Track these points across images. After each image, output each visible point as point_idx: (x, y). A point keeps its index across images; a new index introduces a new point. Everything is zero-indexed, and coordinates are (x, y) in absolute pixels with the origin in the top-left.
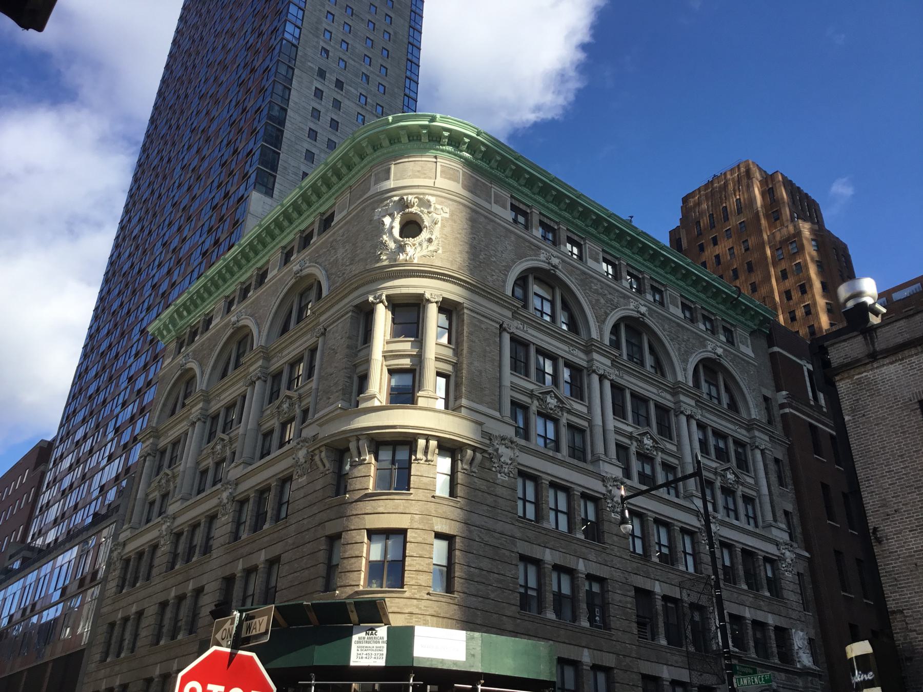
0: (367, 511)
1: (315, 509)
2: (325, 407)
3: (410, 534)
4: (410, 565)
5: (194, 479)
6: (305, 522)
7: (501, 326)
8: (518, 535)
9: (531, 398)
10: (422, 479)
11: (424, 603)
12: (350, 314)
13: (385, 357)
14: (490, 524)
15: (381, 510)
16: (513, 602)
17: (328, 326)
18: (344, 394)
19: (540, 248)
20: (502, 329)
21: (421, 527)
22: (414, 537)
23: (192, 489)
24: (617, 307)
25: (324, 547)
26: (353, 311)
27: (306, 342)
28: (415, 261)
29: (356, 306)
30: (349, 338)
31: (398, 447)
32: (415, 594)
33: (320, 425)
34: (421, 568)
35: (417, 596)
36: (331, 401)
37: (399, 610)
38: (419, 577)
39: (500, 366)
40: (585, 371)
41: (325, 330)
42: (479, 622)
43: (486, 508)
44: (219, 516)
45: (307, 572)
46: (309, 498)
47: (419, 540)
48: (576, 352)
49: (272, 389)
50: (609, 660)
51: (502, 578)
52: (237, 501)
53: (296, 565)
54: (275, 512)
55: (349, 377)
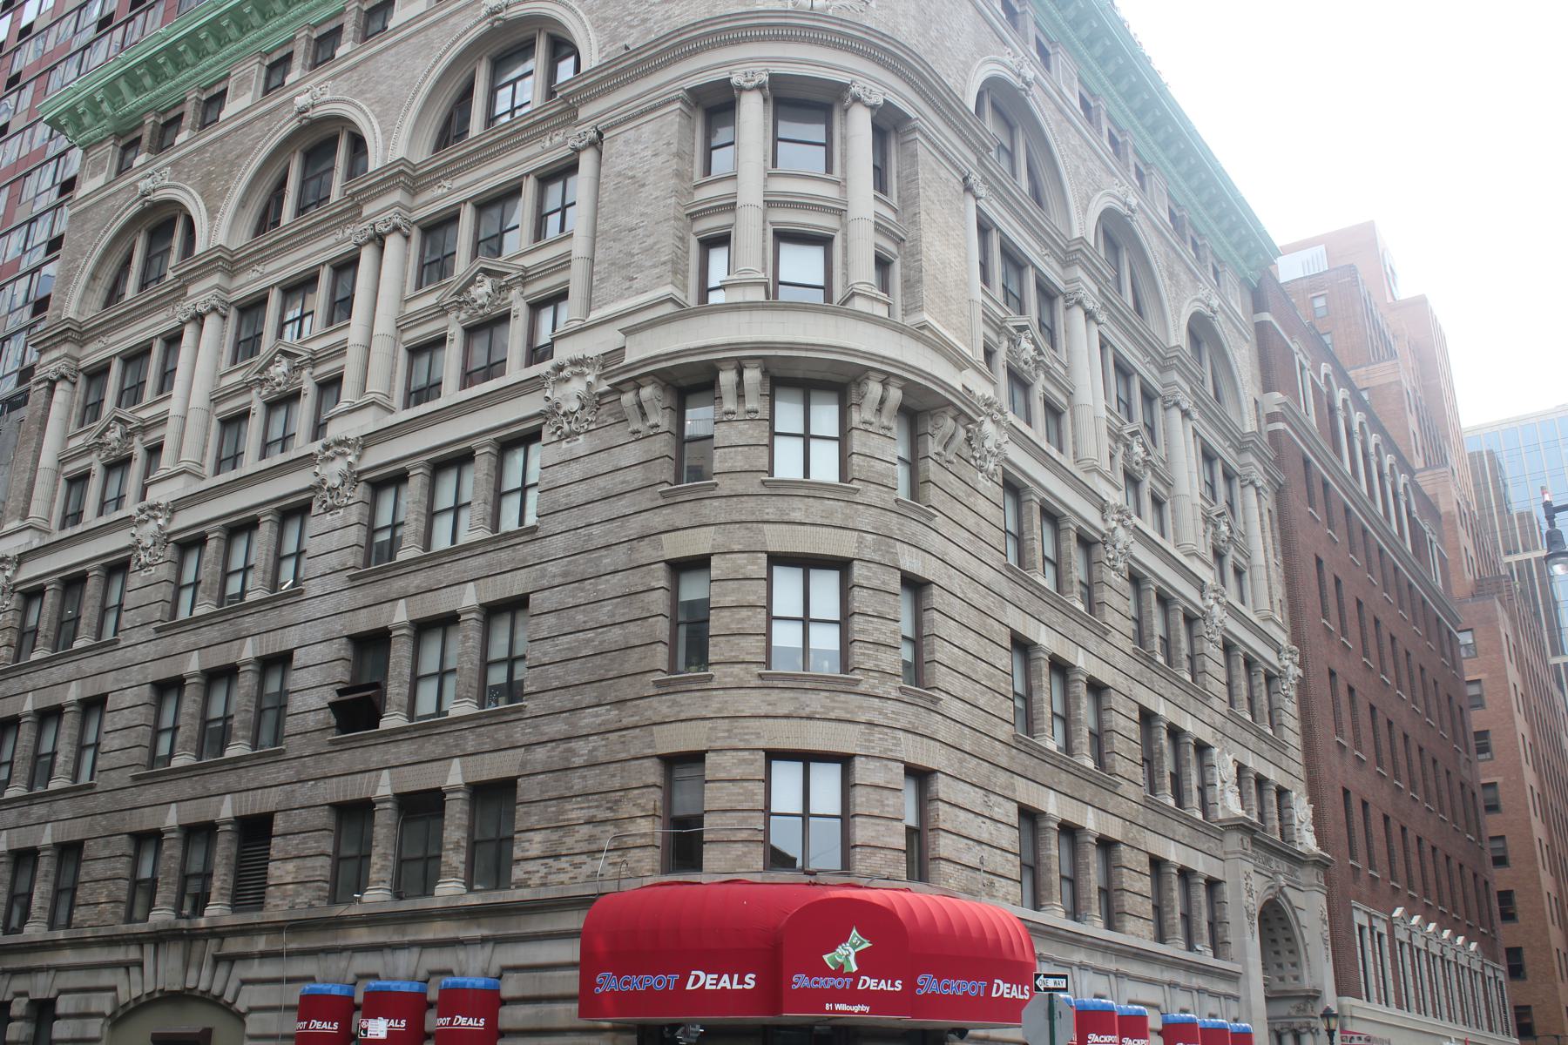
0: (766, 517)
1: (622, 506)
2: (621, 297)
3: (858, 571)
4: (863, 631)
5: (207, 434)
6: (595, 530)
7: (965, 179)
8: (1007, 594)
9: (998, 334)
10: (873, 462)
11: (890, 706)
12: (678, 105)
13: (769, 204)
14: (973, 566)
15: (797, 516)
16: (1005, 717)
17: (608, 128)
18: (675, 272)
19: (1005, 43)
20: (968, 189)
21: (877, 558)
22: (868, 578)
23: (204, 454)
24: (1099, 189)
25: (662, 583)
26: (683, 101)
27: (529, 159)
28: (830, 12)
29: (690, 91)
31: (814, 396)
32: (873, 687)
33: (627, 332)
34: (882, 639)
35: (879, 692)
36: (636, 284)
37: (848, 716)
38: (881, 655)
39: (967, 261)
40: (1061, 300)
41: (600, 135)
42: (967, 749)
43: (967, 535)
44: (315, 510)
45: (617, 631)
46: (600, 482)
47: (876, 583)
48: (1051, 260)
49: (422, 256)
50: (1114, 830)
51: (992, 670)
53: (580, 617)
54: (489, 509)
55: (682, 239)
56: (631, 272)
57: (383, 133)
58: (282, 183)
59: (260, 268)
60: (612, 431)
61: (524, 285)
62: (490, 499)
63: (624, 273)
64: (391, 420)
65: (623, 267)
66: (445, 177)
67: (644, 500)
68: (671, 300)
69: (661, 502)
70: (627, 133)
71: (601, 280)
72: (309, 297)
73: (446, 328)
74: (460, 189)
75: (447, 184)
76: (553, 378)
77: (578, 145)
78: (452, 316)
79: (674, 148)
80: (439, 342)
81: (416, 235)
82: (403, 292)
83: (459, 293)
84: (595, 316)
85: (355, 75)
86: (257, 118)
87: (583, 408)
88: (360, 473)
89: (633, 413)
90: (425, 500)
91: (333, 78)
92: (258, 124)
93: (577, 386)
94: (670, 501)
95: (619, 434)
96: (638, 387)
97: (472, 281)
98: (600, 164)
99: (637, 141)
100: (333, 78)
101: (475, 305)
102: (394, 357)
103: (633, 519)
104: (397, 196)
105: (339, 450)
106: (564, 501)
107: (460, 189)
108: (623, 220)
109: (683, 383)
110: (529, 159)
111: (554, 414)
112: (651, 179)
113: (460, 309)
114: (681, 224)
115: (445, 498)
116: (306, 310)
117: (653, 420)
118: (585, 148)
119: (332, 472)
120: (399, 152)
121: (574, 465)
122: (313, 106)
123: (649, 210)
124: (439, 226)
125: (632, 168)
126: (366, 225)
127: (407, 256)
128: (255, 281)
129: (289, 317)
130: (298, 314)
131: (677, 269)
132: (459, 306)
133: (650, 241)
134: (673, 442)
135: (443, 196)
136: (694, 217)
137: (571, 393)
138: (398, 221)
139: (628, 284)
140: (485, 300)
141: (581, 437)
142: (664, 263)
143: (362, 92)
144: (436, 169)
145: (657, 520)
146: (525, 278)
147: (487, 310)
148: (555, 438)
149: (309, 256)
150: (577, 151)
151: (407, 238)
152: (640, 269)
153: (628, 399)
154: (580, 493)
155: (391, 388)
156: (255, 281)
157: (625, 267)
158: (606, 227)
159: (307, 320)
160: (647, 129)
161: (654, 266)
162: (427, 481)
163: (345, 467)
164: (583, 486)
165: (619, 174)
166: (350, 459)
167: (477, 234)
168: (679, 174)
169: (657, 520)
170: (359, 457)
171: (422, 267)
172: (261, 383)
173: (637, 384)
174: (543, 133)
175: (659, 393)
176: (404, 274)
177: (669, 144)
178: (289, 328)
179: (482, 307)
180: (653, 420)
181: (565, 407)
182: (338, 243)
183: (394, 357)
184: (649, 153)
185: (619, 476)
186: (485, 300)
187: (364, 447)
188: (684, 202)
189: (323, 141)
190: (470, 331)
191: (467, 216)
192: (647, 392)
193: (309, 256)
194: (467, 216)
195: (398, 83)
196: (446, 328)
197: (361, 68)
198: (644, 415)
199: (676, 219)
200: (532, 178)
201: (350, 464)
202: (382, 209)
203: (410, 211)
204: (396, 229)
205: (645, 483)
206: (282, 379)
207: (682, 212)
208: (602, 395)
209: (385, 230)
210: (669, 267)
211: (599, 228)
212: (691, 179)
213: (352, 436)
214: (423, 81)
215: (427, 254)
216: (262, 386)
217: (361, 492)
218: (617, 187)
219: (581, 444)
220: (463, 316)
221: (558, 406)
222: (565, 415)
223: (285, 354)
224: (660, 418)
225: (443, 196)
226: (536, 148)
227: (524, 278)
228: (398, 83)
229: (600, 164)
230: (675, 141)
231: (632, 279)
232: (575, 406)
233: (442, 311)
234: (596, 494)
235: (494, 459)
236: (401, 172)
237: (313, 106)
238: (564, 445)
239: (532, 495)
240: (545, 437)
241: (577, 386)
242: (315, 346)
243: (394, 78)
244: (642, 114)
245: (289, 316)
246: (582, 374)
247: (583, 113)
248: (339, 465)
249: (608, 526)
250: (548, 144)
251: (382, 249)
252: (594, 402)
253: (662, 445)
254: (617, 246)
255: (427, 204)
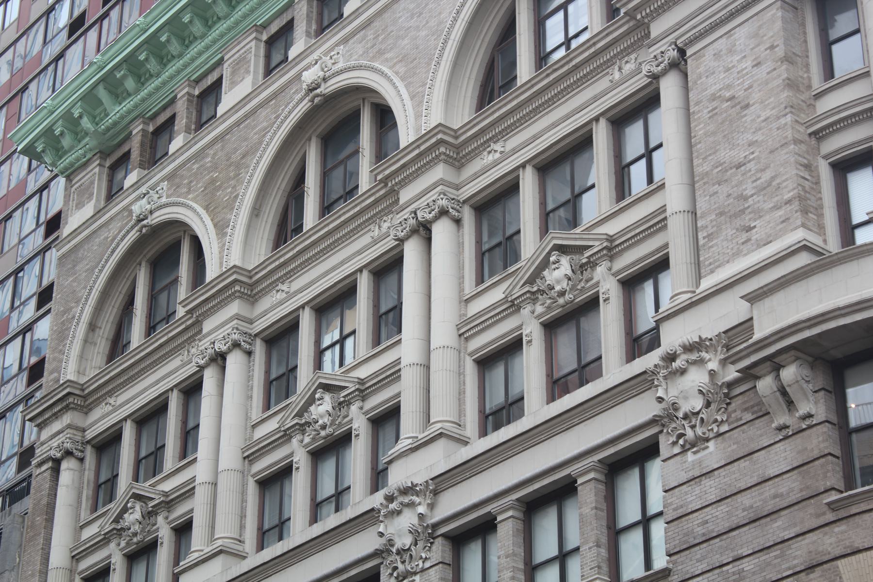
1: (778, 529)
2: (737, 254)
5: (243, 501)
17: (691, 42)
18: (805, 211)
23: (242, 527)
27: (595, 99)
30: (788, 59)
33: (753, 298)
36: (755, 235)
41: (682, 52)
46: (745, 500)
49: (479, 242)
52: (444, 536)
54: (604, 552)
55: (807, 167)
56: (746, 220)
57: (412, 98)
58: (300, 180)
59: (284, 287)
60: (752, 431)
61: (611, 258)
62: (604, 540)
63: (738, 222)
64: (465, 453)
65: (736, 215)
66: (495, 139)
67: (807, 517)
68: (805, 248)
69: (830, 517)
70: (717, 42)
71: (709, 237)
72: (348, 313)
73: (520, 327)
74: (514, 151)
75: (498, 147)
76: (663, 372)
77: (656, 70)
78: (526, 311)
79: (780, 52)
80: (513, 347)
81: (468, 216)
82: (461, 290)
83: (531, 281)
84: (707, 283)
85: (370, 33)
86: (261, 105)
87: (708, 404)
88: (435, 526)
89: (775, 403)
90: (521, 551)
91: (345, 40)
92: (263, 113)
93: (696, 378)
94: (843, 513)
95: (760, 434)
96: (777, 368)
97: (545, 264)
98: (686, 89)
99: (731, 51)
100: (345, 40)
101: (553, 293)
102: (461, 374)
103: (795, 544)
104: (439, 172)
105: (406, 500)
106: (700, 530)
107: (514, 151)
108: (726, 155)
109: (838, 354)
110: (595, 99)
111: (672, 418)
112: (756, 96)
113: (534, 301)
114: (803, 147)
115: (546, 546)
116: (347, 331)
117: (804, 408)
118: (664, 72)
119: (401, 528)
120: (436, 117)
121: (707, 482)
122: (325, 80)
123: (759, 137)
124: (497, 199)
125: (728, 87)
126: (405, 214)
127: (460, 245)
128: (281, 303)
129: (327, 341)
130: (337, 336)
131: (807, 205)
132: (533, 297)
133: (766, 176)
134: (835, 434)
135: (496, 163)
136: (819, 135)
137: (689, 388)
138: (444, 203)
139: (744, 236)
140: (564, 284)
141: (711, 444)
142: (789, 202)
143: (381, 53)
144: (482, 131)
145: (828, 542)
146: (612, 249)
147: (568, 297)
148: (677, 450)
149: (342, 263)
150: (655, 78)
151: (458, 222)
152: (758, 214)
153: (765, 385)
154: (719, 518)
155: (461, 412)
156: (281, 303)
157: (740, 216)
158: (706, 167)
159: (349, 343)
160: (741, 34)
161: (777, 207)
162: (520, 525)
163: (415, 521)
164: (723, 507)
165: (713, 98)
166: (421, 509)
167: (543, 203)
168: (791, 84)
169: (828, 542)
170: (432, 506)
171: (481, 255)
172: (302, 428)
173: (775, 364)
174: (609, 64)
175: (806, 372)
176: (460, 267)
177: (772, 47)
178: (328, 355)
179: (562, 294)
180: (804, 408)
181: (685, 407)
182: (375, 242)
183: (461, 374)
184: (748, 63)
185: (768, 490)
186: (564, 284)
187: (436, 493)
188: (804, 118)
189: (343, 120)
190: (551, 327)
191: (528, 182)
192: (789, 373)
193: (342, 263)
194: (528, 182)
195: (423, 33)
196: (520, 327)
197: (376, 24)
198: (790, 404)
199: (796, 141)
200: (603, 122)
201: (421, 517)
202: (421, 192)
203: (457, 187)
204: (443, 212)
205: (806, 494)
206: (326, 420)
207: (803, 132)
208: (730, 385)
209: (429, 217)
210: (796, 205)
211: (698, 170)
212: (809, 87)
213: (419, 479)
214: (452, 26)
215: (485, 238)
216: (303, 432)
217: (439, 550)
218: (713, 113)
219: (712, 454)
220: (539, 309)
221: (675, 407)
222: (686, 417)
223: (327, 388)
224: (813, 406)
225: (496, 163)
226: (603, 84)
227: (609, 249)
228: (423, 33)
229: (686, 89)
230: (780, 42)
231: (749, 229)
232: (697, 403)
233: (513, 306)
234: (741, 516)
235: (602, 487)
236: (441, 142)
237: (325, 80)
238: (690, 457)
239: (658, 529)
240: (665, 449)
241: (696, 378)
242: (363, 373)
243: (418, 29)
244: (732, 15)
245: (327, 341)
246: (701, 362)
247: (657, 29)
248: (408, 520)
249: (763, 557)
250: (617, 75)
251: (429, 240)
252: (722, 395)
253: (820, 440)
254: (724, 189)
255: (476, 176)
